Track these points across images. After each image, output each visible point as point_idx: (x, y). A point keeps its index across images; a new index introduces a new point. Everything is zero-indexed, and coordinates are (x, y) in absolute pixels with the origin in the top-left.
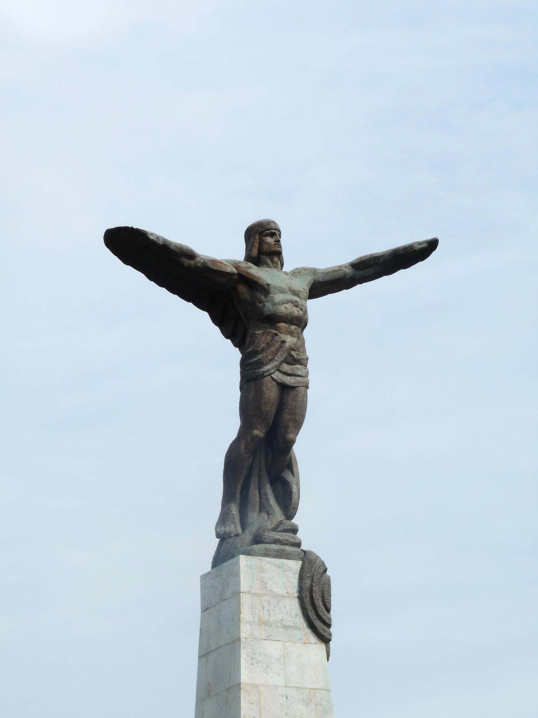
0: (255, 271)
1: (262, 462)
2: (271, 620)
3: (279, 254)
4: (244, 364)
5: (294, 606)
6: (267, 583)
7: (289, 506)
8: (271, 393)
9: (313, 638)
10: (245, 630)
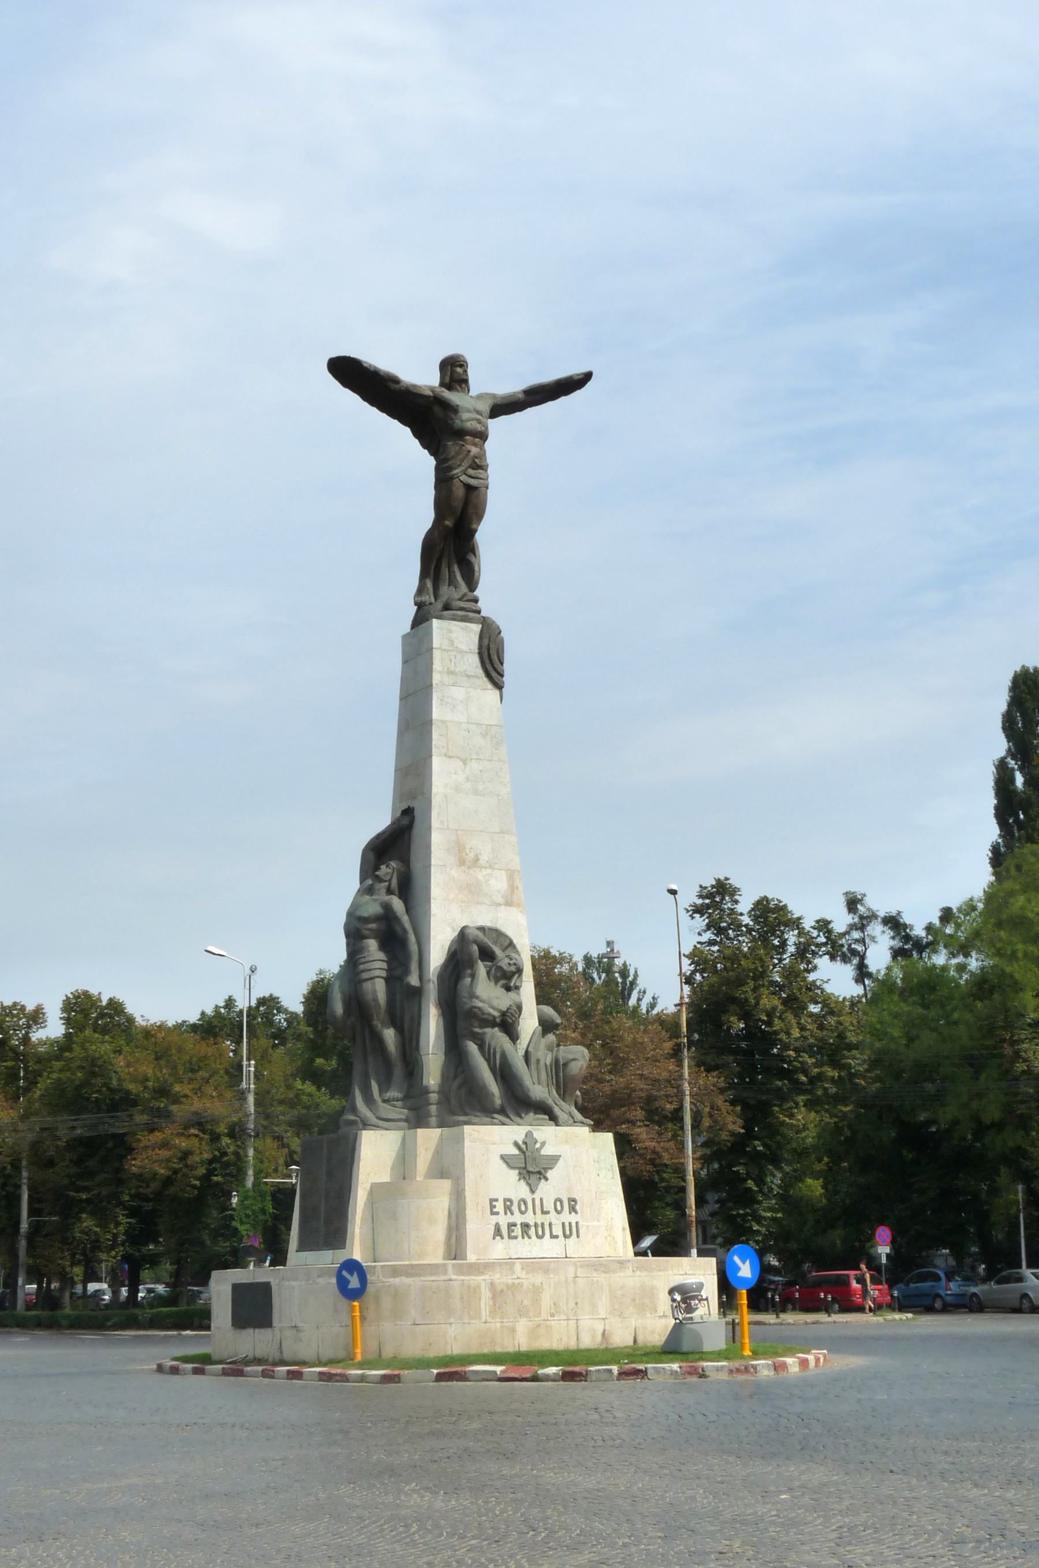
0: (447, 394)
1: (450, 548)
2: (458, 669)
3: (466, 381)
4: (438, 469)
5: (476, 659)
6: (453, 640)
7: (471, 581)
8: (459, 492)
9: (490, 686)
10: (436, 678)
